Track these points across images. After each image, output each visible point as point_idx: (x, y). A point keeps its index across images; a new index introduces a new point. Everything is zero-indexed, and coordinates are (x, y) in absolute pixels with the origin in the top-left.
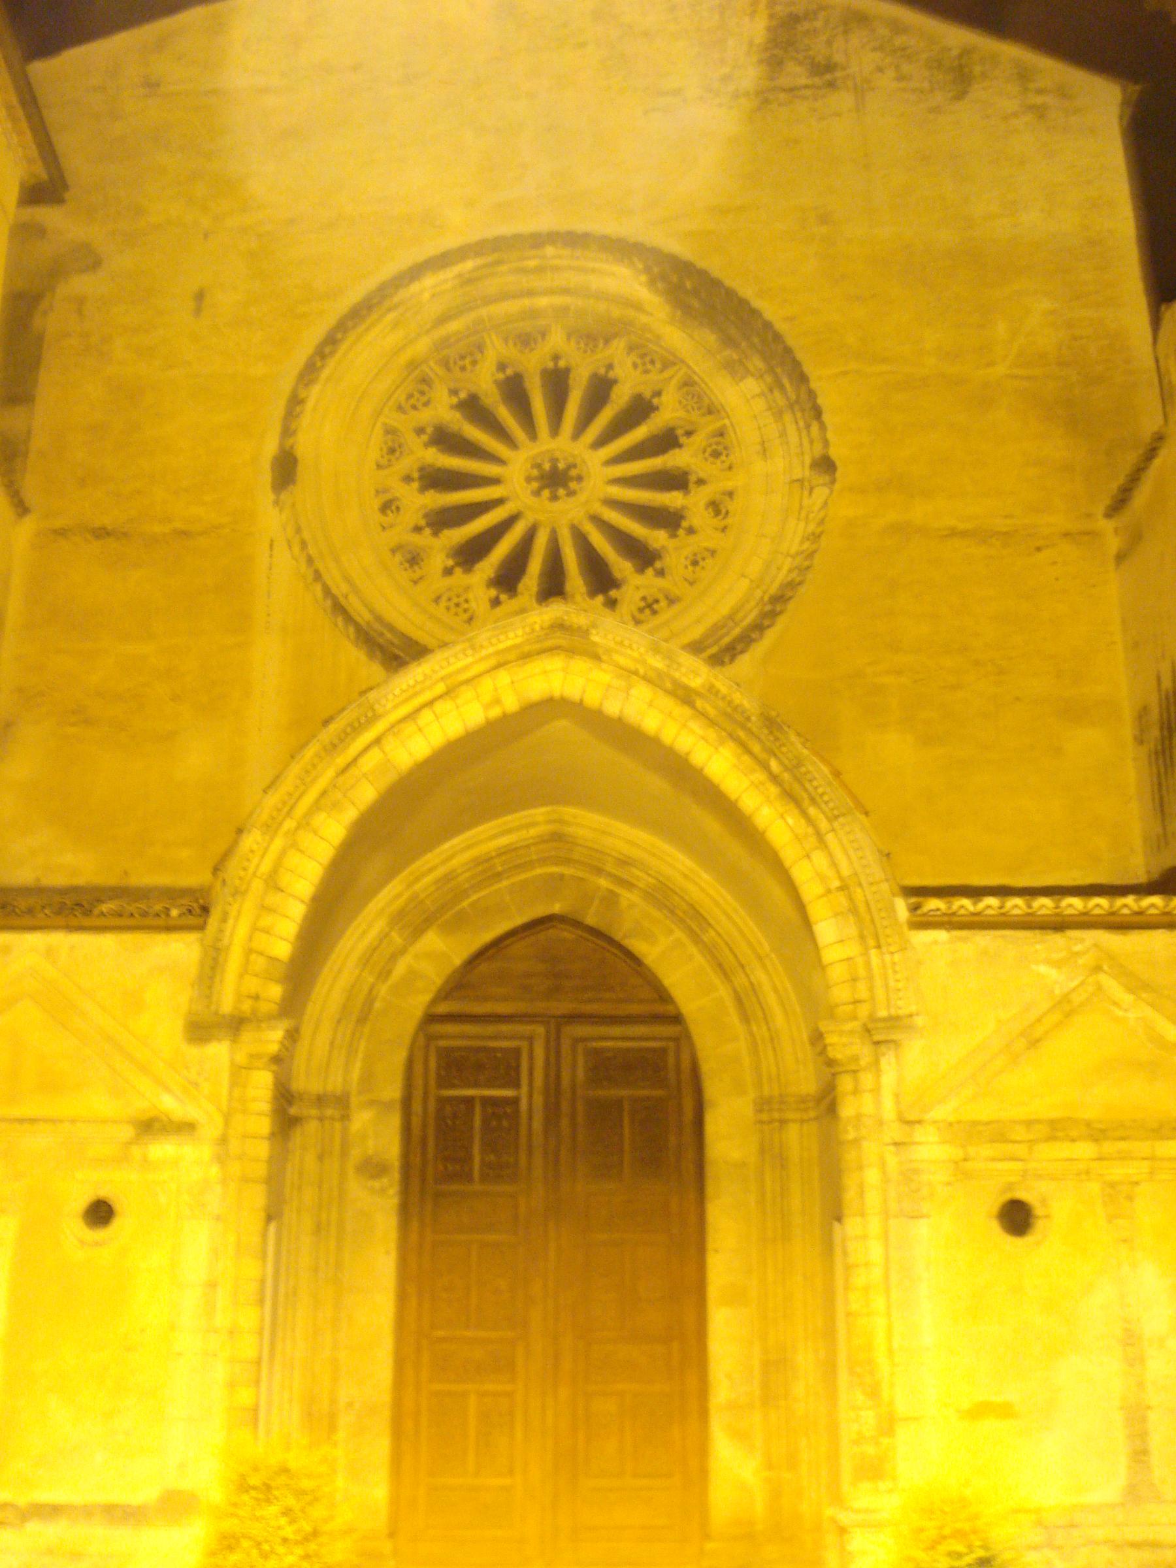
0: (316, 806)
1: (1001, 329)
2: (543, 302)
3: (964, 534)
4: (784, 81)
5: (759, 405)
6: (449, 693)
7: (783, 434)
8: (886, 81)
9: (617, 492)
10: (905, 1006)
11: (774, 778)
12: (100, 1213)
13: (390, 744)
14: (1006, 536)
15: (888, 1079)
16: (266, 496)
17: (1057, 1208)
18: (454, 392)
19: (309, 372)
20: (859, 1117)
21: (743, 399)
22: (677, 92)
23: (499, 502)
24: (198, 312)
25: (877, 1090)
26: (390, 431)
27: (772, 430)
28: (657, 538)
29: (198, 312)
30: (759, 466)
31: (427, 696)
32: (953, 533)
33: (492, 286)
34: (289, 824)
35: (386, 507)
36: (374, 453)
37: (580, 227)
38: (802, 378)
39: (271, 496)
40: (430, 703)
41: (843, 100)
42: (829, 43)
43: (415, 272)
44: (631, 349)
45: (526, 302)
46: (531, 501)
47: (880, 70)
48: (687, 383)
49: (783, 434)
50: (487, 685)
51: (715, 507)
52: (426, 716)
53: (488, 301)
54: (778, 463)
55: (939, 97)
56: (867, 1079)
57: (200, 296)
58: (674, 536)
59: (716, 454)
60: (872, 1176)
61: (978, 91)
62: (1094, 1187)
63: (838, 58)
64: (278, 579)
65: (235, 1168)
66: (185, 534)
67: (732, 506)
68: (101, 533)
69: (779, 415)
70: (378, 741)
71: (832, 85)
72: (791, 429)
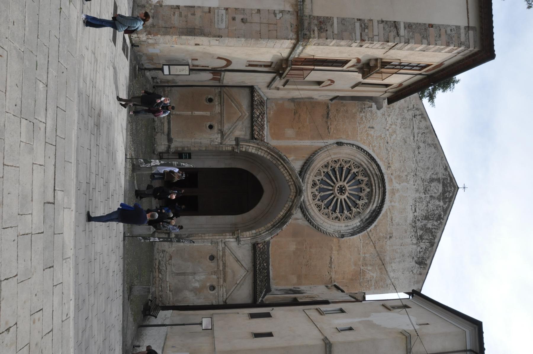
0: (272, 155)
1: (370, 268)
2: (374, 188)
3: (331, 260)
4: (418, 231)
5: (355, 225)
6: (290, 175)
7: (349, 229)
8: (419, 249)
9: (339, 200)
10: (242, 243)
11: (277, 224)
12: (211, 127)
13: (282, 166)
14: (331, 267)
15: (232, 240)
16: (335, 141)
17: (213, 264)
18: (357, 172)
19: (358, 147)
20: (226, 236)
21: (356, 223)
22: (415, 211)
23: (337, 181)
24: (369, 127)
25: (230, 238)
26: (349, 161)
27: (351, 227)
28: (331, 208)
29: (369, 127)
30: (343, 225)
31: (289, 171)
32: (331, 258)
33: (376, 179)
34: (269, 151)
35: (335, 161)
36: (345, 159)
37: (387, 194)
38: (359, 232)
39: (335, 142)
40: (288, 171)
41: (415, 241)
42: (427, 239)
43: (378, 165)
44: (366, 203)
45: (374, 185)
46: (337, 186)
47: (421, 248)
48: (359, 213)
49: (349, 229)
50: (291, 180)
51: (337, 217)
52: (286, 171)
53: (373, 178)
54: (344, 228)
55: (416, 259)
56: (232, 237)
57: (373, 128)
58: (331, 210)
59: (346, 218)
60: (217, 237)
61: (417, 266)
62: (216, 269)
63: (423, 241)
64: (319, 143)
65: (218, 146)
66: (328, 128)
67: (337, 220)
68: (328, 114)
69: (353, 229)
70: (282, 164)
71: (418, 239)
72: (350, 231)
